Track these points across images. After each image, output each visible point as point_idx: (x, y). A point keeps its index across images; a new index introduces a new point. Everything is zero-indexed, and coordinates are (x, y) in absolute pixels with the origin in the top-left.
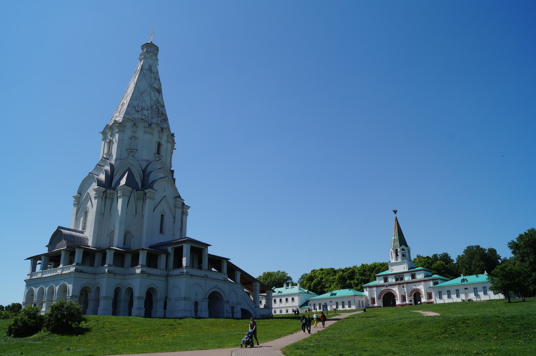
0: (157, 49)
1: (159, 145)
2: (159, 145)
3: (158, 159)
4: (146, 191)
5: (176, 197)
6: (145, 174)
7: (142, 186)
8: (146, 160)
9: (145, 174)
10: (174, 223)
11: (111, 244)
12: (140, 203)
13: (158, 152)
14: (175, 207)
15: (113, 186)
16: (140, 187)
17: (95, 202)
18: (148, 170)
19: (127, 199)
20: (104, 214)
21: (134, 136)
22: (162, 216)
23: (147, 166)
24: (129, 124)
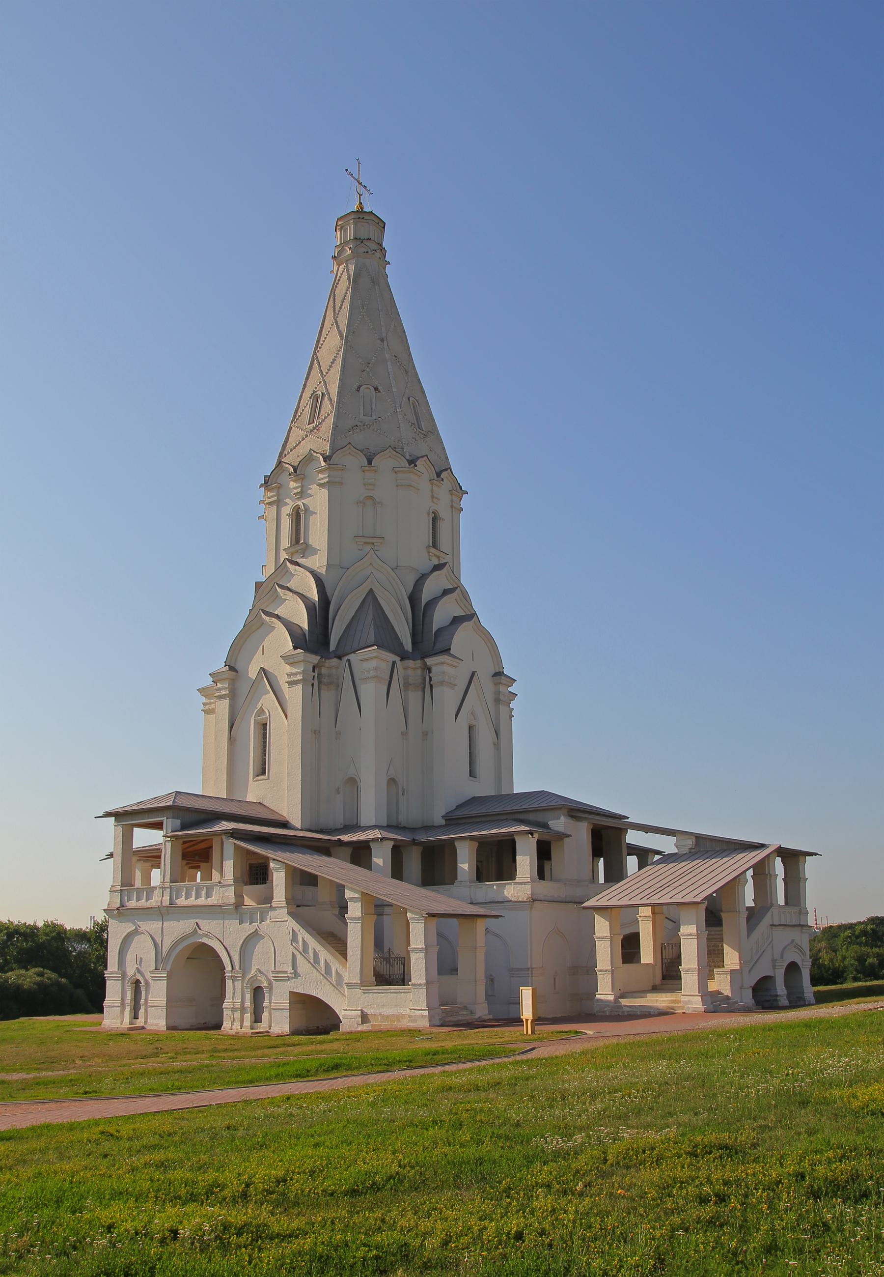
1: (435, 520)
2: (435, 520)
4: (430, 661)
6: (419, 611)
7: (414, 643)
9: (419, 611)
12: (414, 697)
15: (332, 647)
16: (408, 647)
18: (426, 595)
21: (371, 498)
22: (470, 728)
24: (353, 461)
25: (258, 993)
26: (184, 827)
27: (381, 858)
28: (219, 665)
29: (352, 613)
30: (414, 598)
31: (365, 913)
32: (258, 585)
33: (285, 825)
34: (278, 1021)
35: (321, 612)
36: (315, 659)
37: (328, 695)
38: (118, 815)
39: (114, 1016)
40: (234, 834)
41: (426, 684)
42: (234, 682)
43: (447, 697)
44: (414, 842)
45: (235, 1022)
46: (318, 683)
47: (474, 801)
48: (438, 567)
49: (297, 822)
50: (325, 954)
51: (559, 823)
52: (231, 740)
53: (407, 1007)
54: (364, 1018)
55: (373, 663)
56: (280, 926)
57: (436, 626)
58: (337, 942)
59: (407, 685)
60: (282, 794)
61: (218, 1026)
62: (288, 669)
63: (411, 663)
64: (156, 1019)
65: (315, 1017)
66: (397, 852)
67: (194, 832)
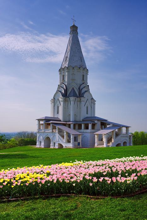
0: (77, 28)
1: (83, 76)
2: (83, 76)
3: (83, 82)
4: (81, 98)
5: (92, 99)
7: (79, 95)
8: (79, 84)
10: (91, 109)
11: (70, 118)
12: (79, 103)
13: (83, 80)
14: (92, 103)
16: (78, 96)
17: (62, 103)
18: (81, 88)
19: (74, 102)
20: (65, 109)
23: (80, 86)
24: (71, 68)
25: (54, 143)
26: (46, 122)
27: (72, 126)
28: (52, 98)
29: (70, 91)
30: (79, 89)
31: (66, 134)
32: (59, 85)
33: (60, 121)
34: (57, 147)
35: (66, 91)
36: (65, 98)
37: (67, 103)
38: (38, 120)
39: (38, 146)
40: (52, 123)
41: (80, 101)
42: (54, 100)
43: (83, 103)
44: (77, 124)
45: (52, 147)
46: (65, 101)
47: (87, 117)
48: (83, 83)
49: (62, 120)
50: (62, 139)
51: (96, 122)
52: (54, 108)
53: (70, 145)
54: (66, 147)
55: (72, 99)
56: (57, 135)
57: (82, 93)
58: (63, 137)
59: (78, 101)
60: (60, 116)
61: (50, 147)
62: (61, 99)
63: (78, 98)
64: (42, 146)
65: (61, 146)
66: (74, 125)
67: (47, 122)
